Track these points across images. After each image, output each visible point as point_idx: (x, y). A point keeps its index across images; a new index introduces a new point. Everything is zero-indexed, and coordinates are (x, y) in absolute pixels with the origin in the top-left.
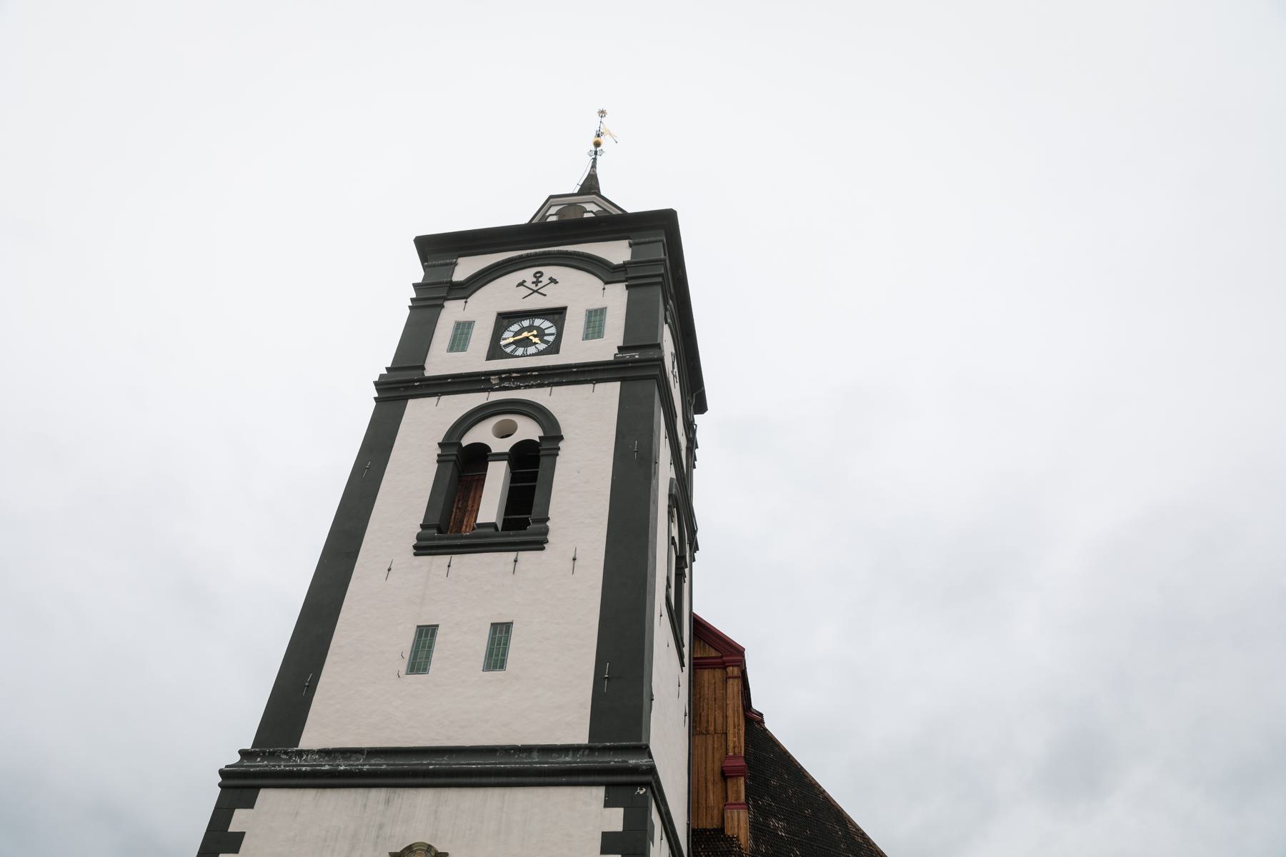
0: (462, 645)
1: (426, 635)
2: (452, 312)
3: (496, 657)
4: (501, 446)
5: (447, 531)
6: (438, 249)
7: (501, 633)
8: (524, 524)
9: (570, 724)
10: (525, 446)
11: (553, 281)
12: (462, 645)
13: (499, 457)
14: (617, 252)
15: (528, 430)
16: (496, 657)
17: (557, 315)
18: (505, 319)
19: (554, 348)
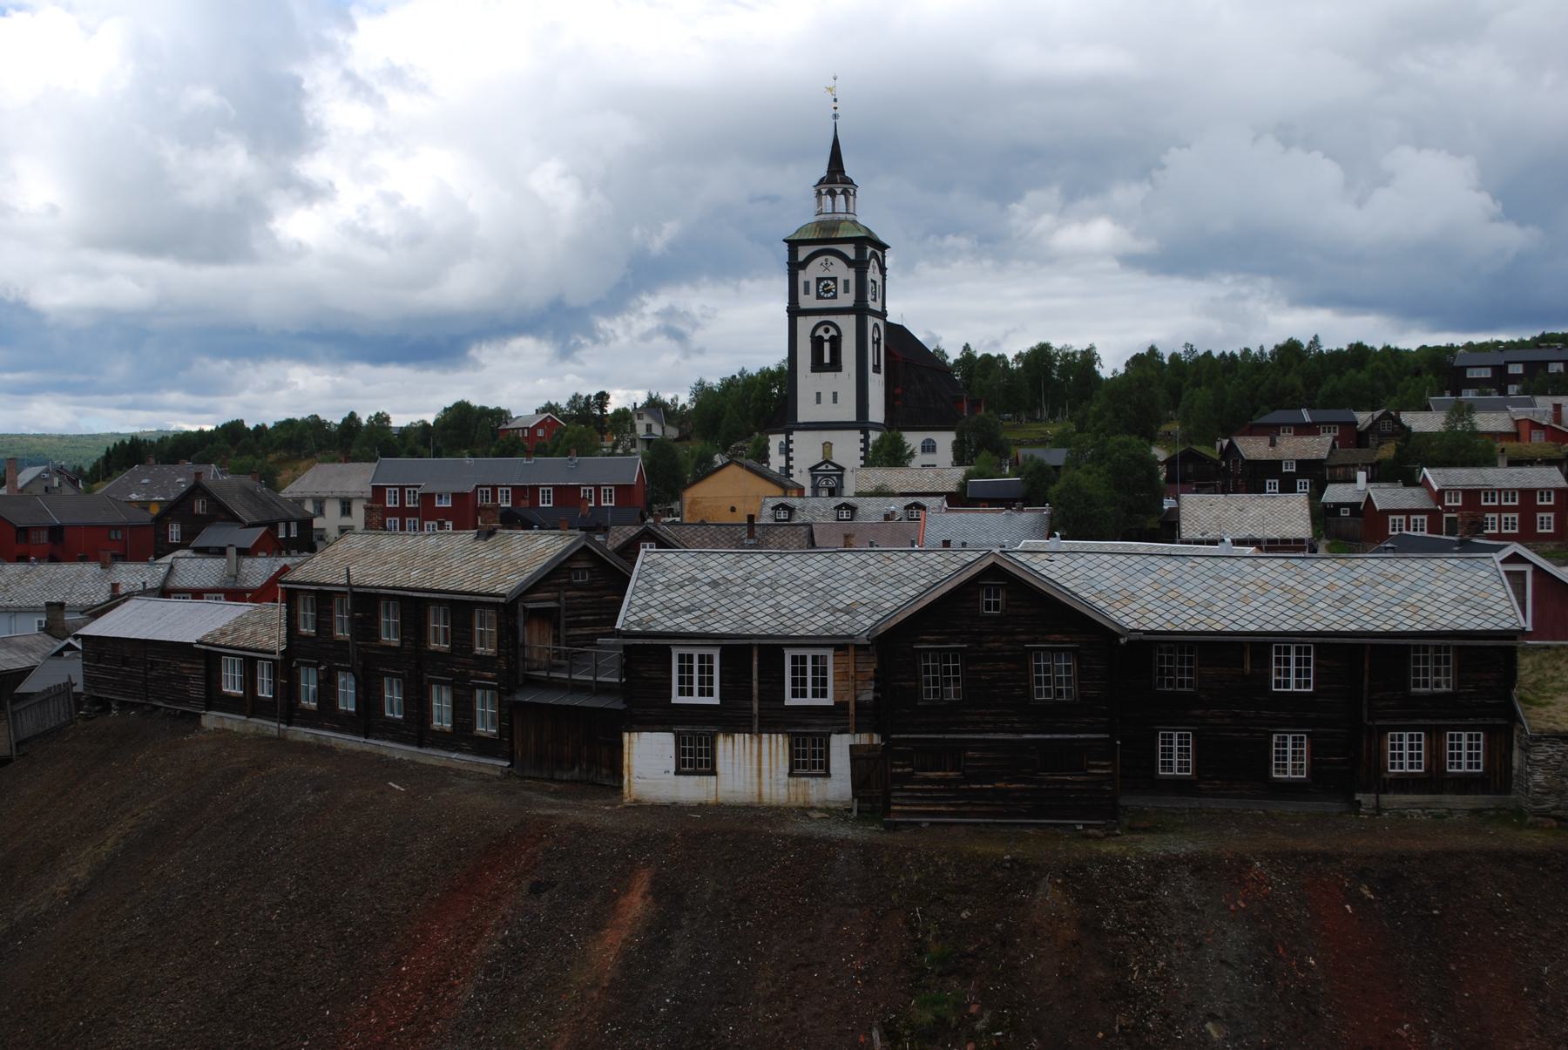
0: (827, 397)
1: (819, 394)
2: (802, 276)
3: (835, 401)
4: (826, 337)
5: (818, 366)
6: (793, 244)
7: (835, 394)
8: (836, 365)
9: (850, 415)
12: (827, 397)
14: (849, 250)
15: (833, 332)
16: (835, 401)
17: (834, 280)
18: (819, 280)
19: (835, 297)
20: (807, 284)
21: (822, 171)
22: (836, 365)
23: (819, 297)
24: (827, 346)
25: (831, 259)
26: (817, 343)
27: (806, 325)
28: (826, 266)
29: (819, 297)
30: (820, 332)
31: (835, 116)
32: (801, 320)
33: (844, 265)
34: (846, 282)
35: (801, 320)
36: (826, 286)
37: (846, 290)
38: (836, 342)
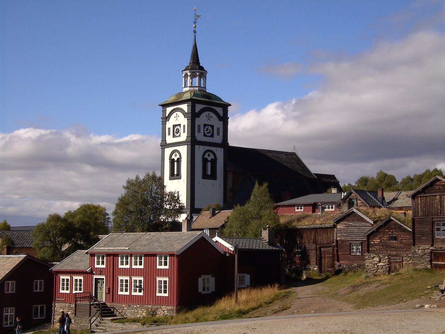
4: (209, 159)
5: (205, 176)
10: (212, 159)
11: (211, 117)
13: (209, 161)
14: (220, 110)
15: (212, 157)
17: (212, 127)
18: (205, 125)
19: (212, 136)
20: (199, 126)
21: (187, 61)
22: (213, 176)
23: (205, 135)
24: (209, 164)
25: (212, 114)
26: (205, 161)
27: (200, 150)
28: (209, 118)
29: (205, 135)
30: (206, 156)
31: (195, 32)
32: (197, 147)
33: (218, 119)
34: (218, 129)
35: (197, 147)
36: (210, 129)
37: (218, 134)
38: (214, 162)
